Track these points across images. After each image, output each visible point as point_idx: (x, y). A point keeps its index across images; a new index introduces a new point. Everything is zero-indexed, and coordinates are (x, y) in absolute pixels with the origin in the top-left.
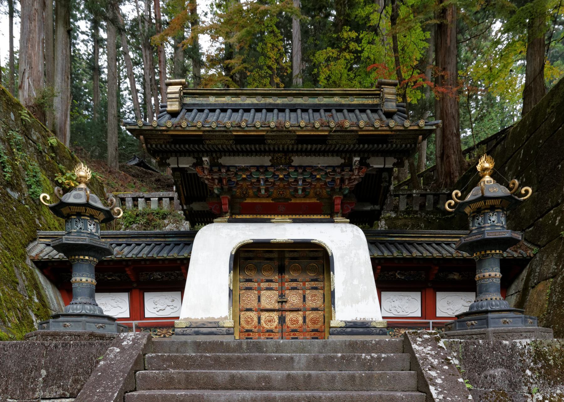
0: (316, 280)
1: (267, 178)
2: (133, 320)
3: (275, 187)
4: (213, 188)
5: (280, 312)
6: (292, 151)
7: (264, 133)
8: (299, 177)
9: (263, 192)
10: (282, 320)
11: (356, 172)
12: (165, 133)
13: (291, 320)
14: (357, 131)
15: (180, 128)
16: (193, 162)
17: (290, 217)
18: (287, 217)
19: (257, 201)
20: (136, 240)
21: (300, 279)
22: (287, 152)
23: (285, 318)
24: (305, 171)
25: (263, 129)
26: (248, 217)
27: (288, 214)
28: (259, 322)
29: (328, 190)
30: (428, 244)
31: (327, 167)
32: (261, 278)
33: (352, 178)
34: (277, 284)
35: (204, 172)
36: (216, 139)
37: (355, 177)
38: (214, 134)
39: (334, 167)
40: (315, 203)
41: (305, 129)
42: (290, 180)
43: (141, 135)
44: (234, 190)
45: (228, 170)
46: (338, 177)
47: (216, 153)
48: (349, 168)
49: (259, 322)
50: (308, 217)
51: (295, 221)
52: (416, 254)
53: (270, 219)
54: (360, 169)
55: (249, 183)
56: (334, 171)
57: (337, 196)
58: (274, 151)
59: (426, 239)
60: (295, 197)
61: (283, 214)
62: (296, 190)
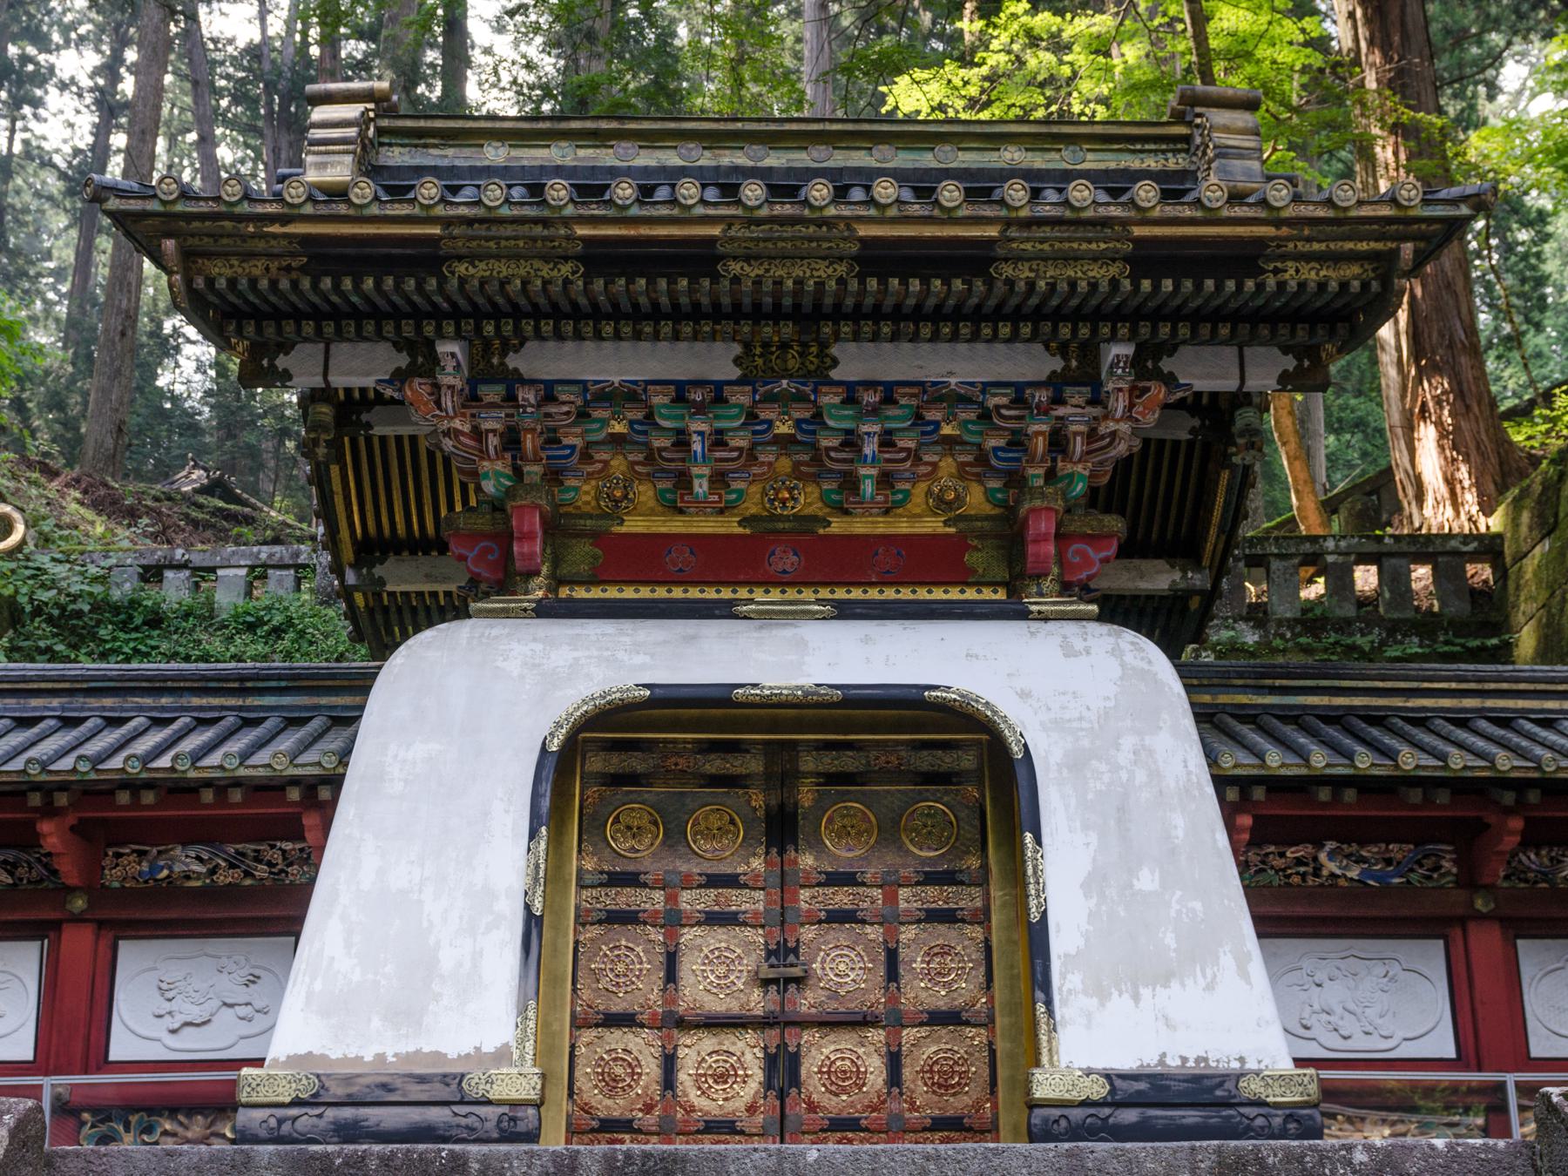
0: (948, 878)
1: (720, 432)
2: (46, 1074)
3: (755, 470)
4: (475, 474)
5: (774, 1033)
6: (837, 314)
7: (716, 231)
8: (865, 428)
9: (701, 487)
10: (783, 1070)
11: (1120, 405)
12: (275, 229)
13: (828, 1071)
14: (1125, 223)
15: (342, 209)
16: (391, 367)
17: (824, 593)
18: (808, 594)
19: (676, 526)
20: (108, 702)
21: (870, 874)
22: (815, 319)
23: (795, 1060)
24: (889, 400)
25: (711, 212)
26: (629, 593)
27: (815, 584)
28: (669, 1080)
29: (994, 484)
30: (1462, 723)
31: (986, 386)
32: (684, 868)
33: (1102, 430)
34: (759, 895)
35: (438, 403)
36: (498, 257)
37: (1112, 426)
38: (495, 231)
39: (1019, 387)
40: (934, 537)
41: (893, 212)
42: (825, 443)
43: (169, 235)
44: (573, 483)
45: (549, 397)
46: (1039, 427)
47: (499, 320)
48: (1086, 390)
49: (669, 1080)
50: (906, 594)
51: (845, 612)
52: (1409, 760)
53: (731, 603)
54: (1136, 392)
55: (640, 457)
56: (1019, 401)
57: (1038, 503)
58: (757, 314)
59: (1446, 703)
60: (846, 512)
61: (791, 584)
62: (850, 483)
